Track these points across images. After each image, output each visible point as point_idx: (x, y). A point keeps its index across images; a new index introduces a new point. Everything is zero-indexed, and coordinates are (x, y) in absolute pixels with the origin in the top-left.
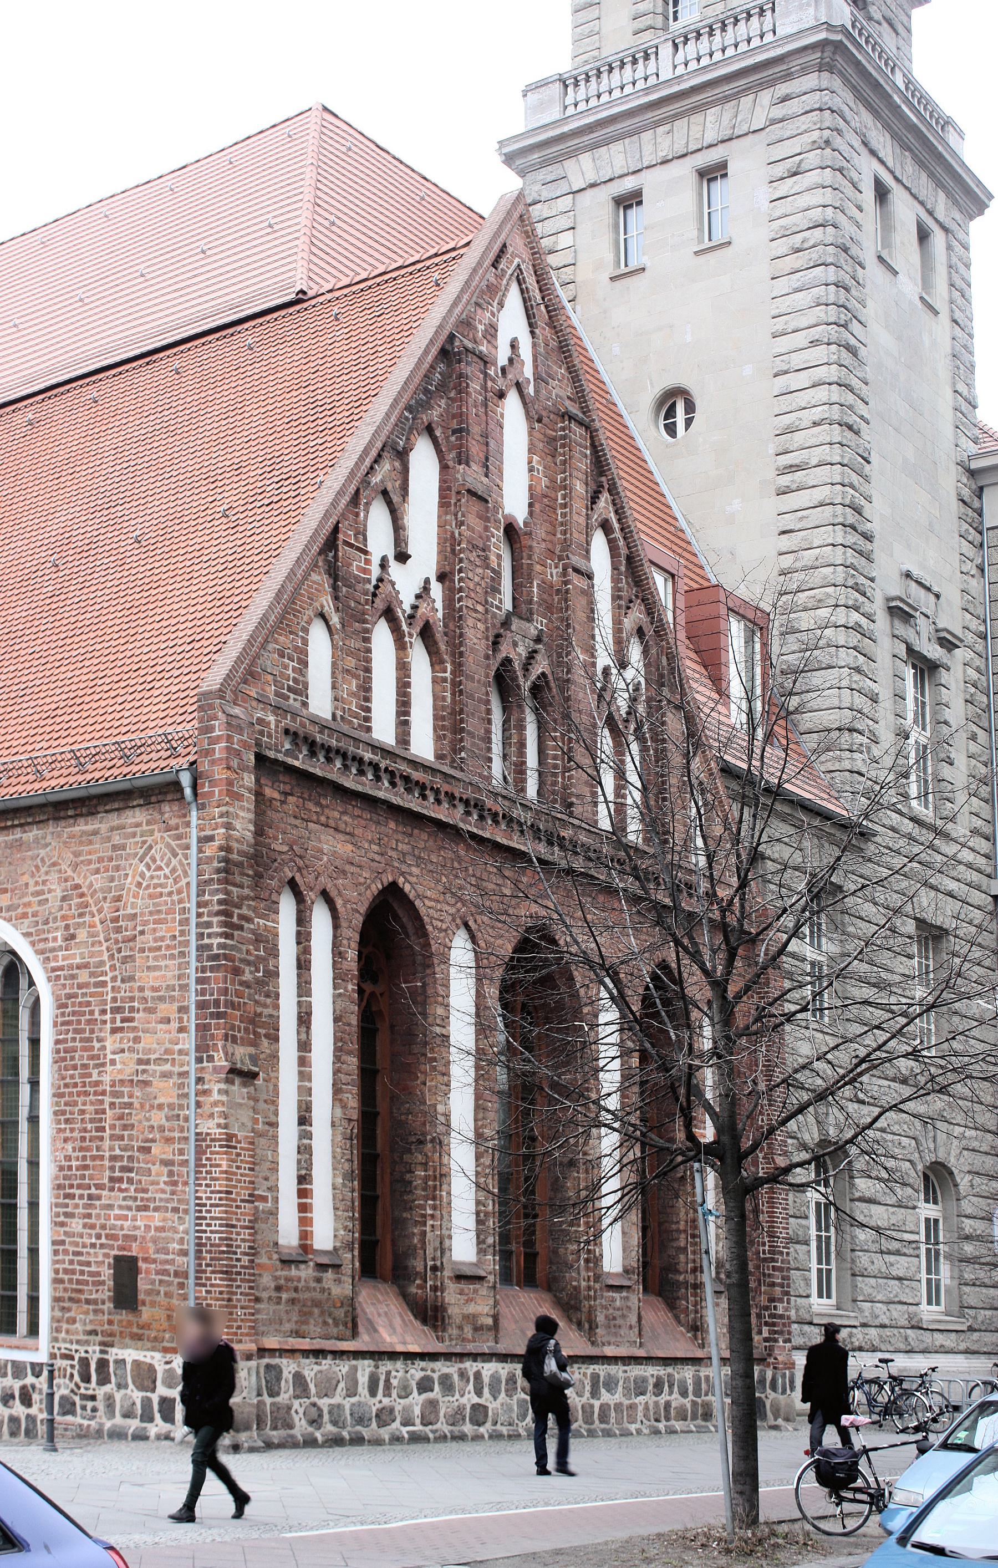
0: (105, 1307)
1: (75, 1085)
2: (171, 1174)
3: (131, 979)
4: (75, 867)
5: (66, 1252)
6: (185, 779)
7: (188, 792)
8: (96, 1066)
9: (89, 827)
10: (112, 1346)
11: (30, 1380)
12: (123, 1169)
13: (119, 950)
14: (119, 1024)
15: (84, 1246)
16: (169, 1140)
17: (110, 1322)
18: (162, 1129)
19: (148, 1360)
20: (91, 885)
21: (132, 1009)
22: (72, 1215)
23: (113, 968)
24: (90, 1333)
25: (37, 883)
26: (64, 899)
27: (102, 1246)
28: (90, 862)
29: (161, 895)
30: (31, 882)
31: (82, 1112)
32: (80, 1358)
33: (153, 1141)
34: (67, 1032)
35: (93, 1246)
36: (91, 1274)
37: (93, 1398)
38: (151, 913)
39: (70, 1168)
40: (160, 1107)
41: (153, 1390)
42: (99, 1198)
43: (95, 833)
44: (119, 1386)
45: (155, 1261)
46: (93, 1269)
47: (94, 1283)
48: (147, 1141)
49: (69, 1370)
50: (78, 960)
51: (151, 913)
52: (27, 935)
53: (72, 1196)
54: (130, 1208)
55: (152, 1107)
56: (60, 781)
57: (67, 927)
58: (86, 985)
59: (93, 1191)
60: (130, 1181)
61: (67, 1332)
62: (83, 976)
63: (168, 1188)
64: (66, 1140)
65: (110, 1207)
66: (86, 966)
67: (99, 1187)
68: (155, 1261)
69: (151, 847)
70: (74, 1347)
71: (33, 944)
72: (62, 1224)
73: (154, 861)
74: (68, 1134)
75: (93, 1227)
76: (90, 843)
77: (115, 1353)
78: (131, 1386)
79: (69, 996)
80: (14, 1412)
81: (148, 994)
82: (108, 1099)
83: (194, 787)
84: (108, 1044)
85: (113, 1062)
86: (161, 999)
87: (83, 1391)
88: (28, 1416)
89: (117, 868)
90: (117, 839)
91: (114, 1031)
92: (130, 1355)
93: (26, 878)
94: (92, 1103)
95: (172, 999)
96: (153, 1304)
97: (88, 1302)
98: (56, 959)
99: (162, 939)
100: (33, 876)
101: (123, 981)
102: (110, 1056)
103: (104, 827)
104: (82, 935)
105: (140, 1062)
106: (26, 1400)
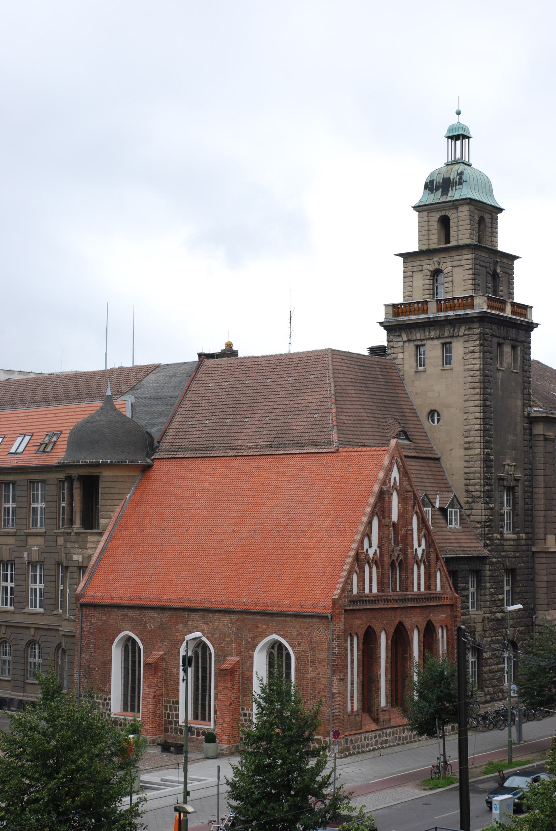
3: (315, 656)
4: (300, 628)
6: (330, 617)
12: (313, 697)
16: (325, 692)
40: (323, 684)
43: (306, 622)
52: (287, 642)
62: (303, 653)
66: (303, 651)
83: (332, 618)
90: (311, 624)
91: (311, 666)
93: (287, 629)
103: (308, 621)
104: (302, 644)
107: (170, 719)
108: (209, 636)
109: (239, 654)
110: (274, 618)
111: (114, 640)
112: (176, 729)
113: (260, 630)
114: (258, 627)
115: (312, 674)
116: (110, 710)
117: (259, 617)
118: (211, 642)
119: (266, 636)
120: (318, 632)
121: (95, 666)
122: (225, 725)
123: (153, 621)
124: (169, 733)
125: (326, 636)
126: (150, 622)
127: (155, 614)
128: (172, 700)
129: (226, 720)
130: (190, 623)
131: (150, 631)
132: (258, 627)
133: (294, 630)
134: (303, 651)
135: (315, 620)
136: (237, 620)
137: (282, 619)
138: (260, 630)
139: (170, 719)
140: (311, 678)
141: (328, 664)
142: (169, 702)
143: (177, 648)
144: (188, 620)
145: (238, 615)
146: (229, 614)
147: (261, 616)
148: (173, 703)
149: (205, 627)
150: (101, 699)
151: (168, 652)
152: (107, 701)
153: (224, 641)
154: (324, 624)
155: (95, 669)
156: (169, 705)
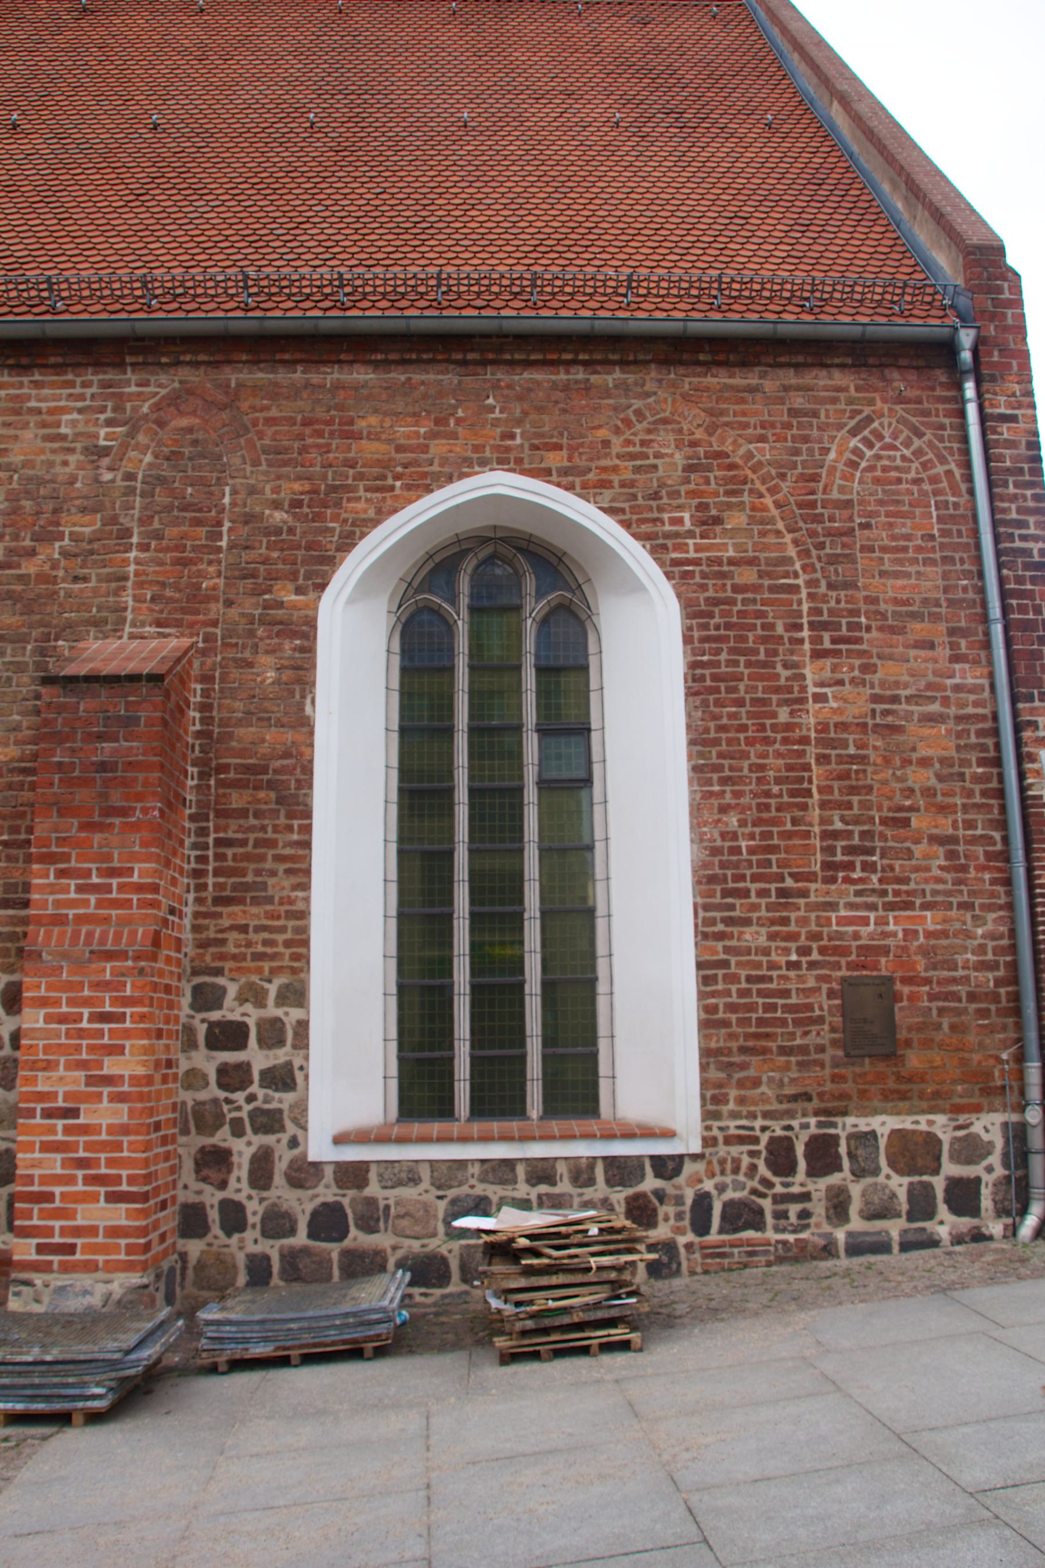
0: (826, 1057)
1: (743, 728)
2: (951, 855)
4: (711, 430)
5: (734, 979)
7: (966, 356)
8: (787, 702)
9: (737, 381)
10: (844, 1113)
11: (650, 1183)
12: (849, 850)
13: (821, 546)
14: (827, 644)
15: (773, 966)
16: (944, 809)
17: (835, 1078)
18: (929, 792)
19: (923, 1127)
20: (749, 455)
21: (854, 627)
22: (747, 922)
24: (794, 1098)
25: (628, 442)
26: (689, 469)
27: (812, 965)
28: (745, 426)
29: (899, 481)
30: (617, 442)
31: (762, 768)
32: (772, 1140)
33: (911, 809)
34: (718, 652)
35: (792, 965)
36: (788, 1008)
37: (806, 1197)
38: (880, 503)
39: (736, 850)
40: (925, 762)
41: (936, 1171)
42: (804, 893)
44: (858, 1174)
45: (928, 981)
46: (793, 1000)
47: (797, 1022)
48: (900, 809)
49: (746, 1161)
50: (731, 553)
51: (880, 503)
52: (609, 511)
53: (746, 893)
54: (873, 907)
55: (906, 762)
57: (702, 507)
58: (756, 588)
59: (789, 883)
61: (741, 1101)
62: (747, 576)
63: (948, 877)
64: (724, 809)
65: (833, 906)
66: (752, 562)
67: (811, 877)
68: (928, 981)
69: (869, 420)
71: (626, 525)
72: (720, 936)
73: (880, 437)
74: (728, 799)
75: (793, 937)
76: (743, 401)
78: (885, 1169)
81: (883, 607)
82: (812, 752)
83: (975, 352)
84: (807, 672)
85: (820, 698)
86: (914, 616)
87: (779, 1189)
89: (806, 439)
90: (799, 401)
91: (818, 654)
92: (884, 1124)
94: (779, 755)
95: (935, 618)
96: (927, 1044)
97: (783, 1051)
99: (908, 537)
100: (617, 431)
101: (831, 586)
102: (812, 689)
103: (769, 385)
104: (737, 520)
105: (876, 699)
109: (181, 606)
110: (491, 374)
113: (371, 449)
117: (362, 375)
119: (424, 484)
120: (854, 442)
122: (104, 1114)
125: (925, 466)
133: (665, 438)
134: (752, 562)
135: (821, 379)
138: (371, 449)
140: (823, 727)
141: (952, 632)
146: (98, 365)
147: (376, 364)
154: (900, 400)
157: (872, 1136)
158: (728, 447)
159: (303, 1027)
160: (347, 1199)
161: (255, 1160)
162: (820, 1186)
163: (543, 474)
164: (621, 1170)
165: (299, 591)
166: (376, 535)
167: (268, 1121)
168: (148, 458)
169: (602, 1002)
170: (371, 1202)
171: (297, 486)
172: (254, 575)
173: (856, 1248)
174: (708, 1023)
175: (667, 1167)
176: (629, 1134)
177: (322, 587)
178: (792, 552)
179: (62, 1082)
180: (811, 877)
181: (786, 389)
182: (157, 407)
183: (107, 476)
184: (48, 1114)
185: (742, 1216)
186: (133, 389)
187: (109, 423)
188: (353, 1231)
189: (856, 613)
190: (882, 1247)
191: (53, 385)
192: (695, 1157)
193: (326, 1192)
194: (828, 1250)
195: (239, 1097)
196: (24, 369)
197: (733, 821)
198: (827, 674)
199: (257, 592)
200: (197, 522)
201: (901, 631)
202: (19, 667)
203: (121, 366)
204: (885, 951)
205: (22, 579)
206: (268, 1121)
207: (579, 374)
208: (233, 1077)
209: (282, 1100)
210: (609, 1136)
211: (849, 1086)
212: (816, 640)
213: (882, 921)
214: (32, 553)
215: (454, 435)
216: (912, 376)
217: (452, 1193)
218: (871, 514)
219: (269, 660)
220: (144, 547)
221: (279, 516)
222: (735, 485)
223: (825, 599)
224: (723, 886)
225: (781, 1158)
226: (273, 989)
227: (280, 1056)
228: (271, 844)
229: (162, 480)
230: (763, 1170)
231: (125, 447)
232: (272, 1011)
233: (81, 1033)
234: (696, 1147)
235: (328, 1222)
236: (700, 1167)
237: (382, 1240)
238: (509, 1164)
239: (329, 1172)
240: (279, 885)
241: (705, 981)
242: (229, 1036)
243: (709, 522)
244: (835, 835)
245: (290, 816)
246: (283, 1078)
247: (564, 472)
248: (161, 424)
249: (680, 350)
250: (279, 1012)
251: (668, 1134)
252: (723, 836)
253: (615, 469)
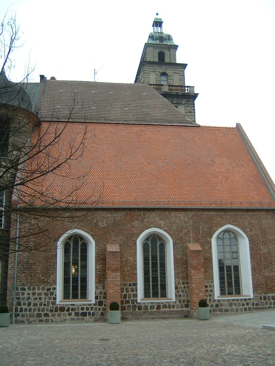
3: (265, 237)
5: (255, 280)
10: (267, 294)
11: (248, 301)
12: (266, 266)
14: (263, 244)
20: (255, 223)
23: (261, 235)
26: (249, 224)
27: (263, 278)
35: (261, 278)
37: (263, 303)
39: (255, 266)
40: (274, 257)
42: (262, 271)
43: (255, 215)
44: (268, 300)
50: (253, 234)
52: (241, 229)
53: (256, 271)
54: (268, 272)
56: (246, 206)
57: (250, 229)
60: (268, 268)
62: (255, 236)
64: (254, 262)
65: (265, 272)
66: (255, 235)
69: (267, 218)
70: (258, 295)
71: (242, 231)
74: (254, 261)
75: (261, 275)
77: (267, 295)
79: (252, 239)
80: (245, 307)
82: (262, 256)
86: (273, 241)
87: (261, 302)
88: (249, 307)
89: (260, 220)
91: (262, 245)
97: (261, 287)
98: (248, 233)
102: (262, 249)
103: (257, 214)
104: (253, 230)
105: (268, 250)
106: (247, 304)
107: (127, 299)
108: (166, 229)
109: (197, 241)
110: (227, 213)
111: (60, 237)
112: (134, 307)
114: (213, 220)
115: (264, 250)
116: (55, 299)
118: (169, 234)
119: (221, 226)
120: (266, 221)
121: (35, 262)
123: (104, 220)
124: (126, 311)
126: (103, 220)
127: (108, 215)
128: (128, 283)
129: (202, 290)
130: (146, 220)
131: (103, 228)
132: (213, 220)
136: (193, 216)
137: (234, 213)
139: (127, 299)
142: (125, 285)
143: (133, 240)
144: (144, 218)
145: (194, 212)
147: (215, 212)
148: (130, 285)
149: (162, 223)
150: (43, 289)
151: (124, 244)
152: (51, 291)
153: (181, 232)
154: (270, 215)
155: (35, 264)
156: (125, 288)
157: (270, 296)
158: (252, 222)
159: (213, 286)
160: (219, 303)
161: (209, 300)
162: (265, 301)
163: (233, 225)
164: (245, 300)
165: (209, 238)
166: (217, 232)
167: (210, 295)
168: (191, 223)
169: (240, 283)
170: (221, 304)
171: (208, 226)
172: (204, 236)
173: (269, 308)
174: (253, 285)
175: (250, 299)
176: (244, 296)
177: (212, 238)
178: (260, 234)
179: (197, 291)
180: (262, 269)
181: (258, 214)
182: (192, 216)
183: (187, 225)
184: (196, 294)
185: (257, 304)
186: (189, 214)
187: (187, 218)
188: (220, 307)
189: (266, 240)
190: (271, 307)
191: (180, 213)
192: (252, 298)
193: (217, 303)
194: (266, 308)
195: (207, 293)
196: (176, 211)
197: (255, 263)
198: (263, 247)
199: (205, 238)
200: (197, 230)
201: (271, 242)
202: (180, 247)
203: (187, 211)
204: (270, 277)
205: (179, 237)
206: (210, 295)
207: (236, 213)
208: (207, 291)
209: (211, 293)
210: (242, 296)
211: (267, 291)
212: (262, 244)
213: (270, 274)
214: (180, 234)
215: (224, 220)
216: (272, 213)
217: (229, 302)
218: (267, 229)
219: (206, 246)
220: (192, 233)
221: (206, 230)
222: (253, 226)
223: (263, 239)
224: (253, 270)
225: (261, 298)
226: (210, 282)
227: (211, 289)
228: (208, 266)
229: (193, 225)
230: (259, 300)
231: (189, 221)
232: (210, 284)
233: (199, 286)
234: (253, 297)
235: (217, 306)
236: (253, 299)
237: (222, 307)
238: (234, 299)
239: (217, 300)
240: (210, 271)
241: (252, 280)
242: (206, 287)
243: (251, 230)
244: (265, 265)
245: (211, 263)
246: (211, 291)
247: (236, 225)
248: (192, 218)
249: (247, 210)
250: (211, 284)
251: (250, 296)
252: (254, 265)
253: (241, 224)
